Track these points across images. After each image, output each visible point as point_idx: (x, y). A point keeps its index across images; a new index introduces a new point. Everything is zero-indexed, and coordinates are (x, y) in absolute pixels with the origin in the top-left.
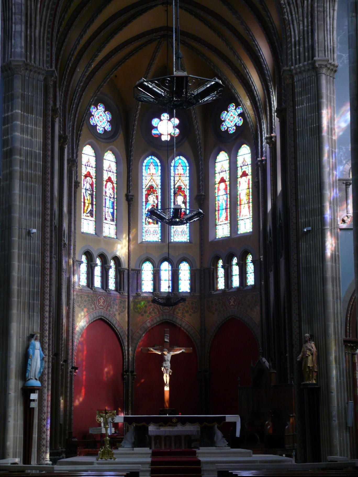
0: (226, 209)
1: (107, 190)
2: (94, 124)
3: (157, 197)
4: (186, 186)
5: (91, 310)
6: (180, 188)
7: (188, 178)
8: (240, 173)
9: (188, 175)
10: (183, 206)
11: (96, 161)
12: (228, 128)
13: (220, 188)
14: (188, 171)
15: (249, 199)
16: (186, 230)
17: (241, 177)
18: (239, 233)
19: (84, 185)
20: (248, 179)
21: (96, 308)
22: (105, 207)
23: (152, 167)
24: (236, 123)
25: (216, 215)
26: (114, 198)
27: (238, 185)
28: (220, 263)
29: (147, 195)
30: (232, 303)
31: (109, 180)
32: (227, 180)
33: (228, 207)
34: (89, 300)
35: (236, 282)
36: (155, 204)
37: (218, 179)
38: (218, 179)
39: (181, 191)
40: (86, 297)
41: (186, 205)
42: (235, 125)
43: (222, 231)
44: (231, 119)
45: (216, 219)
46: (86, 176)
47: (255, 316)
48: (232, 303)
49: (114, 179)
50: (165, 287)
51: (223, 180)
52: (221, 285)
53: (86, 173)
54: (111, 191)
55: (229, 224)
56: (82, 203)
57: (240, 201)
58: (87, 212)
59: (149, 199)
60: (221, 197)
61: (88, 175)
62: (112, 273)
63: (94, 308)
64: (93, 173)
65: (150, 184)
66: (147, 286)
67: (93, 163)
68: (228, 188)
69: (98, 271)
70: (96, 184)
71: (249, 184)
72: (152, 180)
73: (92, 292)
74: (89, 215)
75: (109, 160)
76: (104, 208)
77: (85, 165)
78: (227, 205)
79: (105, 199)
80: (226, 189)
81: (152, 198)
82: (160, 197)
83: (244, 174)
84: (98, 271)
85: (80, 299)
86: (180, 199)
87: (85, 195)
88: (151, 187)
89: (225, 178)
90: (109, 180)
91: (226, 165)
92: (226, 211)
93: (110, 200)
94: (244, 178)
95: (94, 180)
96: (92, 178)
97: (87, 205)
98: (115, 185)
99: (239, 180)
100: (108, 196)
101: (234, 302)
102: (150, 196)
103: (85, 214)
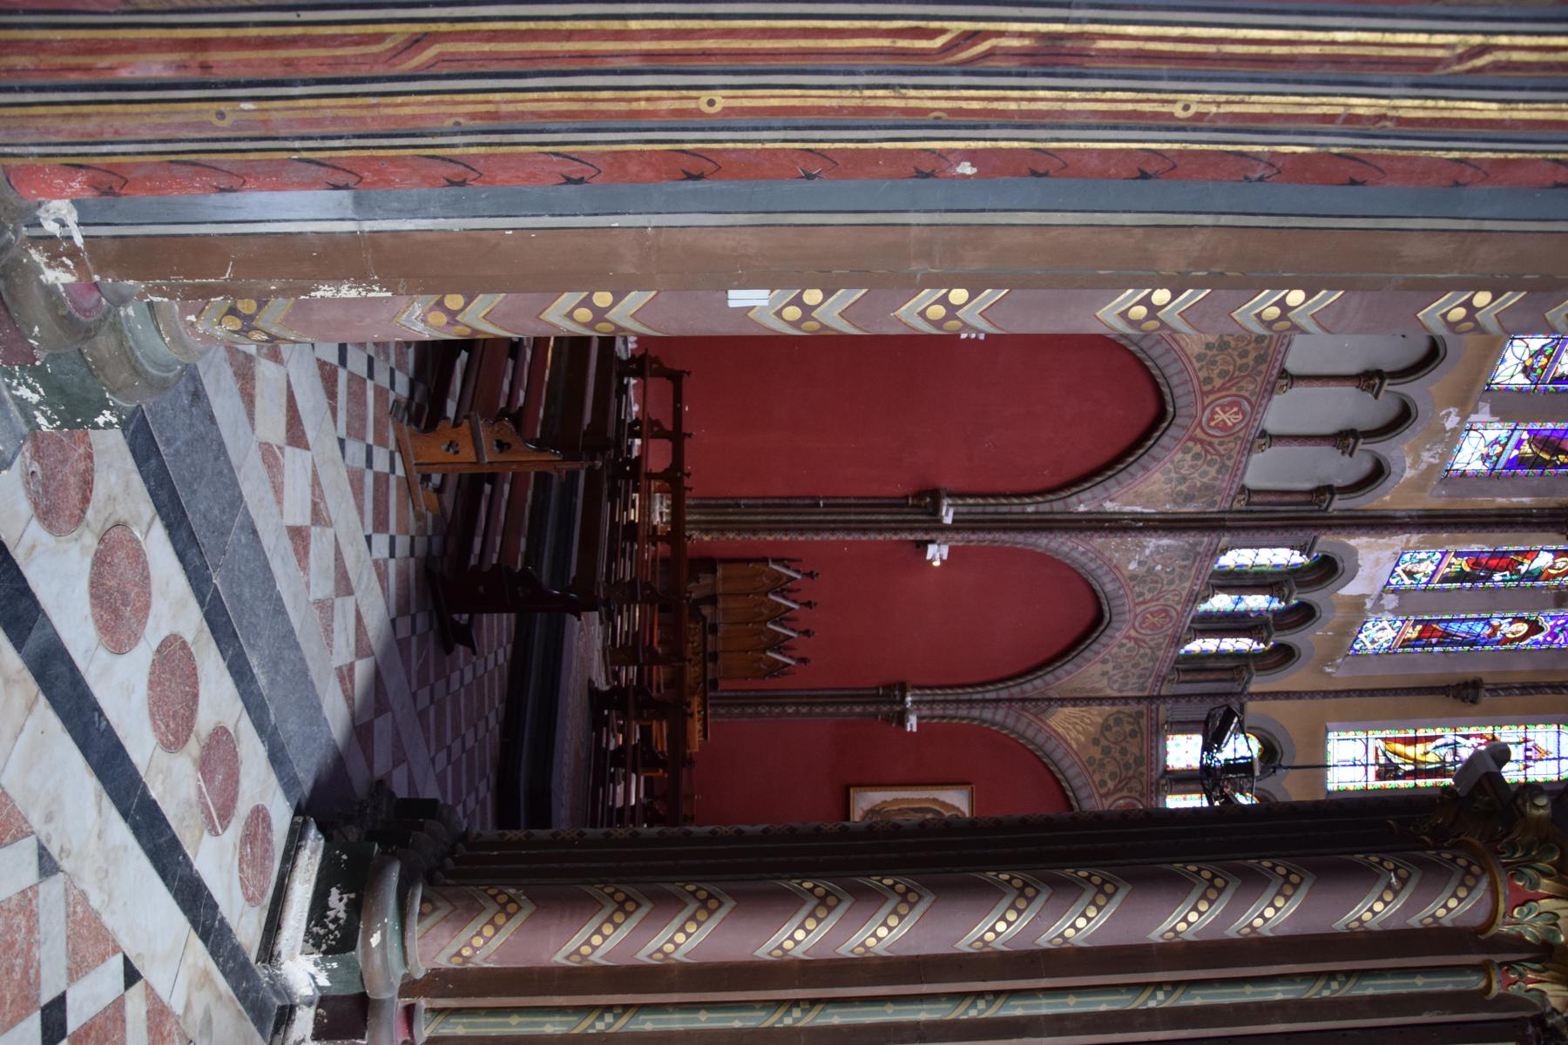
5: (1097, 778)
19: (1467, 737)
21: (1106, 796)
34: (1127, 766)
40: (1136, 751)
56: (1411, 734)
58: (1390, 755)
63: (1103, 791)
73: (1155, 776)
77: (1526, 740)
85: (1128, 728)
87: (1439, 742)
97: (1410, 751)
103: (1381, 744)
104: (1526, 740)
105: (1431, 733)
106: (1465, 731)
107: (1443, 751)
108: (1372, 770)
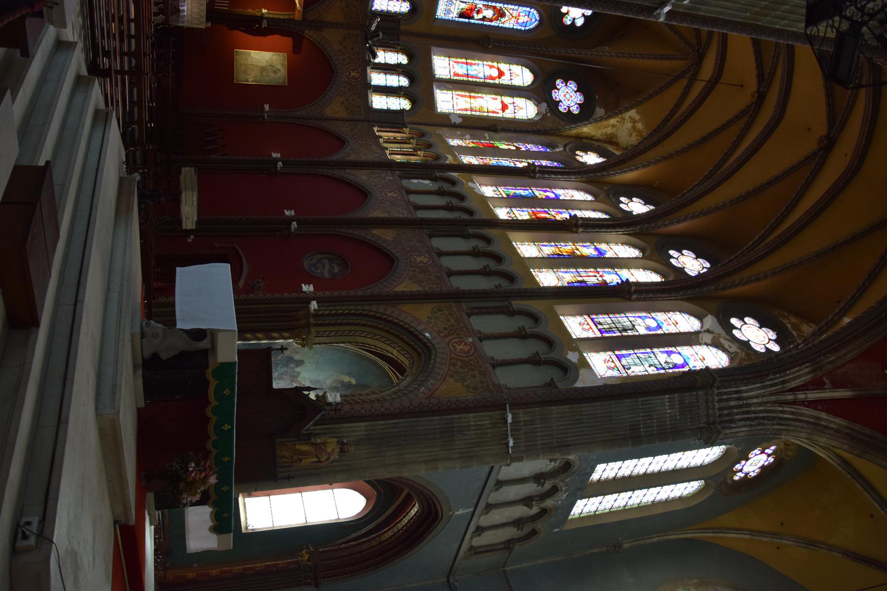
0: (468, 76)
6: (503, 15)
7: (511, 26)
8: (507, 100)
10: (480, 16)
13: (493, 69)
14: (519, 28)
17: (502, 102)
27: (493, 96)
28: (403, 59)
30: (353, 74)
33: (470, 79)
41: (480, 20)
42: (560, 101)
43: (443, 66)
47: (334, 108)
48: (353, 74)
55: (448, 77)
60: (481, 69)
68: (491, 81)
71: (494, 112)
78: (472, 77)
80: (491, 78)
83: (504, 107)
86: (489, 13)
89: (503, 78)
91: (518, 82)
94: (500, 106)
101: (354, 77)
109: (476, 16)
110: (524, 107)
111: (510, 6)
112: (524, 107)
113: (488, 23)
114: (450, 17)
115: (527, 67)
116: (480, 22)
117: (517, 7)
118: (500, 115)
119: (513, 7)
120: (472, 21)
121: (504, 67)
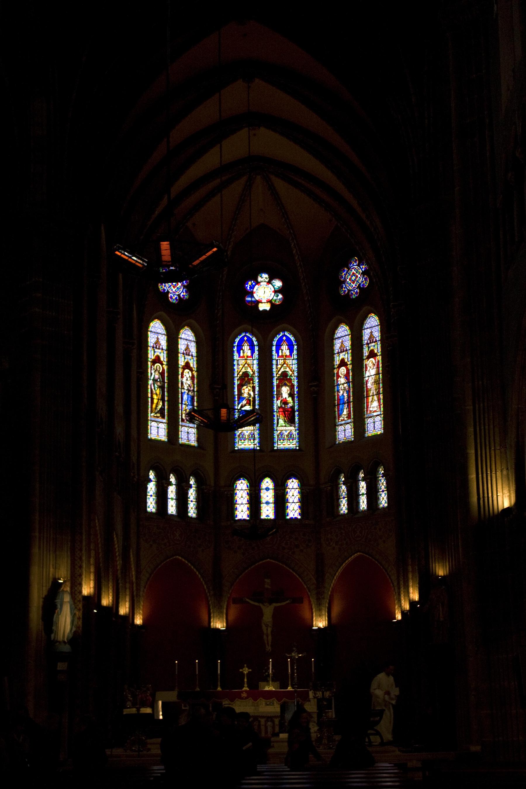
0: (349, 402)
1: (184, 380)
2: (164, 290)
3: (254, 388)
4: (293, 372)
6: (285, 374)
8: (366, 353)
9: (296, 357)
10: (290, 400)
11: (168, 341)
12: (349, 291)
15: (379, 388)
16: (294, 433)
18: (366, 435)
20: (377, 361)
22: (182, 403)
23: (246, 347)
24: (360, 285)
25: (335, 412)
26: (193, 391)
29: (240, 386)
31: (187, 366)
32: (348, 363)
35: (363, 503)
36: (251, 399)
37: (337, 361)
38: (337, 361)
39: (287, 380)
41: (293, 399)
42: (359, 287)
43: (345, 432)
44: (354, 278)
45: (335, 418)
46: (154, 362)
49: (193, 364)
50: (268, 512)
51: (343, 363)
52: (344, 508)
53: (153, 358)
54: (189, 382)
55: (352, 424)
56: (150, 399)
57: (367, 391)
58: (156, 411)
59: (243, 391)
61: (157, 360)
62: (192, 494)
64: (163, 357)
65: (243, 370)
66: (242, 512)
67: (164, 343)
68: (351, 374)
69: (172, 491)
70: (168, 372)
71: (378, 367)
72: (246, 365)
74: (159, 415)
75: (187, 338)
76: (180, 405)
79: (182, 393)
81: (246, 391)
82: (257, 389)
83: (372, 354)
84: (172, 491)
86: (285, 391)
87: (153, 387)
88: (246, 374)
90: (187, 366)
92: (349, 406)
93: (188, 394)
94: (372, 359)
95: (165, 368)
96: (162, 364)
97: (155, 401)
98: (195, 374)
99: (366, 362)
100: (186, 388)
102: (245, 387)
103: (152, 414)
104: (153, 347)
105: (149, 391)
106: (149, 374)
107: (156, 386)
108: (160, 420)
109: (291, 405)
110: (369, 331)
111: (274, 370)
112: (369, 331)
113: (296, 390)
114: (295, 433)
115: (334, 333)
116: (296, 399)
117: (274, 362)
118: (379, 358)
119: (274, 367)
120: (296, 408)
121: (337, 360)
